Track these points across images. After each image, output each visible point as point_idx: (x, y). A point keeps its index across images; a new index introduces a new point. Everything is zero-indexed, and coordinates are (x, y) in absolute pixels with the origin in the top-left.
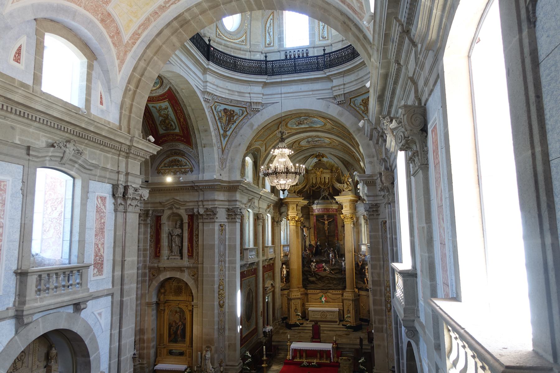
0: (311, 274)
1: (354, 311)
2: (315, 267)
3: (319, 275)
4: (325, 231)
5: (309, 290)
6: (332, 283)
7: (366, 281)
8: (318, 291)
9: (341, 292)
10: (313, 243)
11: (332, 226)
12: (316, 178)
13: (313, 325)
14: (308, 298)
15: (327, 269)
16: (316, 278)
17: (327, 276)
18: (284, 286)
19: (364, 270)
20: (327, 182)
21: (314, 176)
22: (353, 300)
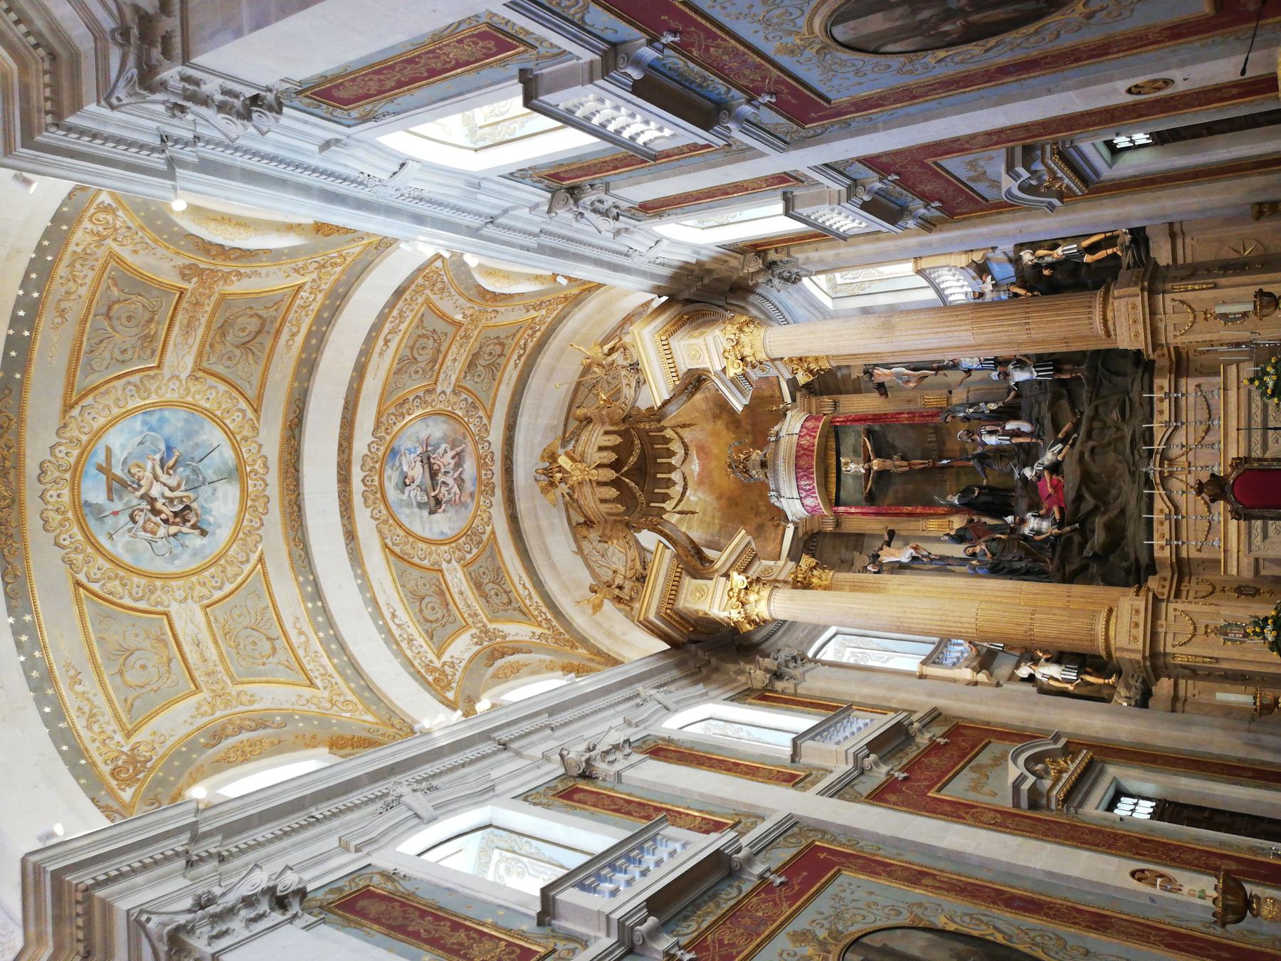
0: (1077, 539)
1: (1222, 281)
2: (1041, 517)
3: (1079, 498)
4: (911, 473)
5: (1157, 554)
6: (1118, 429)
7: (1102, 254)
8: (1159, 504)
9: (1165, 383)
10: (958, 522)
11: (899, 443)
12: (600, 484)
13: (1237, 515)
14: (1203, 561)
15: (1048, 457)
16: (1094, 512)
17: (1082, 455)
18: (1128, 687)
19: (1046, 272)
20: (619, 440)
21: (593, 494)
22: (1152, 292)
